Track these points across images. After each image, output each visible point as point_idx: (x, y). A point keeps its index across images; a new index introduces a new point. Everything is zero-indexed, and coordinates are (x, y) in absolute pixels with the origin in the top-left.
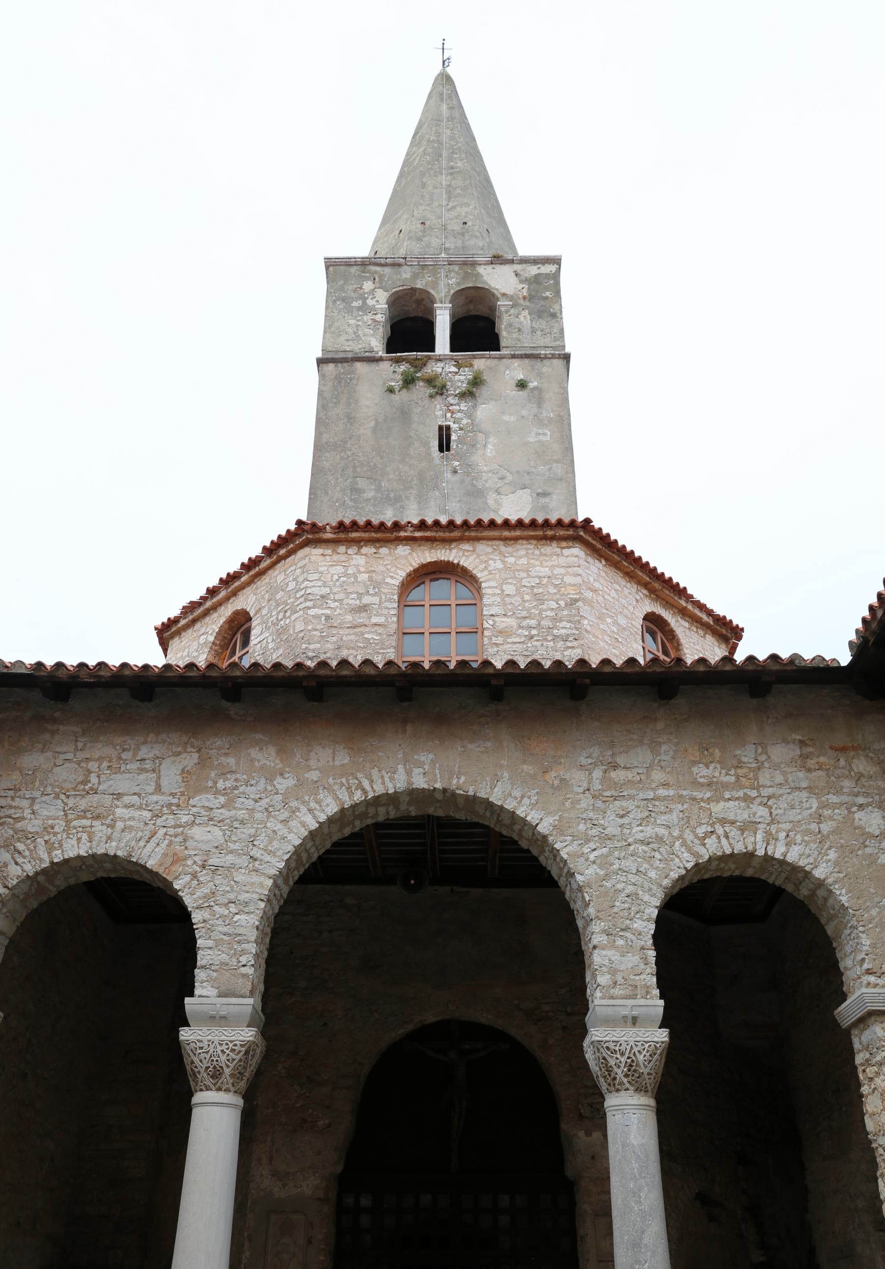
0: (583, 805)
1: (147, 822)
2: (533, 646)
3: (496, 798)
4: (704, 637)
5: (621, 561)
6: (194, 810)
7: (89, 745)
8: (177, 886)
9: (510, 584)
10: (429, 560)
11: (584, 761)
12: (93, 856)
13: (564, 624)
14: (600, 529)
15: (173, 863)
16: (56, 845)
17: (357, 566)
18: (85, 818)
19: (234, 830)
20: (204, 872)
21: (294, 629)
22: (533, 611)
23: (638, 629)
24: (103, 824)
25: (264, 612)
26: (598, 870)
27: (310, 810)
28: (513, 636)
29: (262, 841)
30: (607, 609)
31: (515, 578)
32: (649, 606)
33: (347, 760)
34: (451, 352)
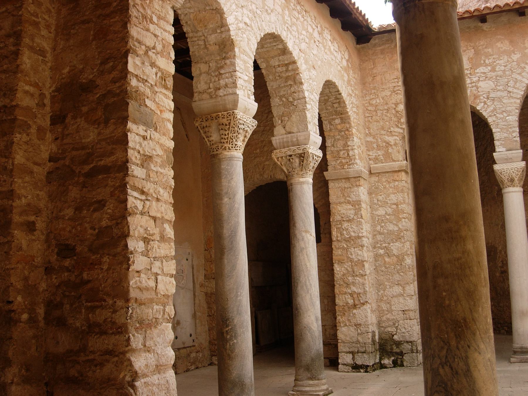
8: (478, 108)
15: (475, 99)
20: (489, 101)
29: (511, 83)
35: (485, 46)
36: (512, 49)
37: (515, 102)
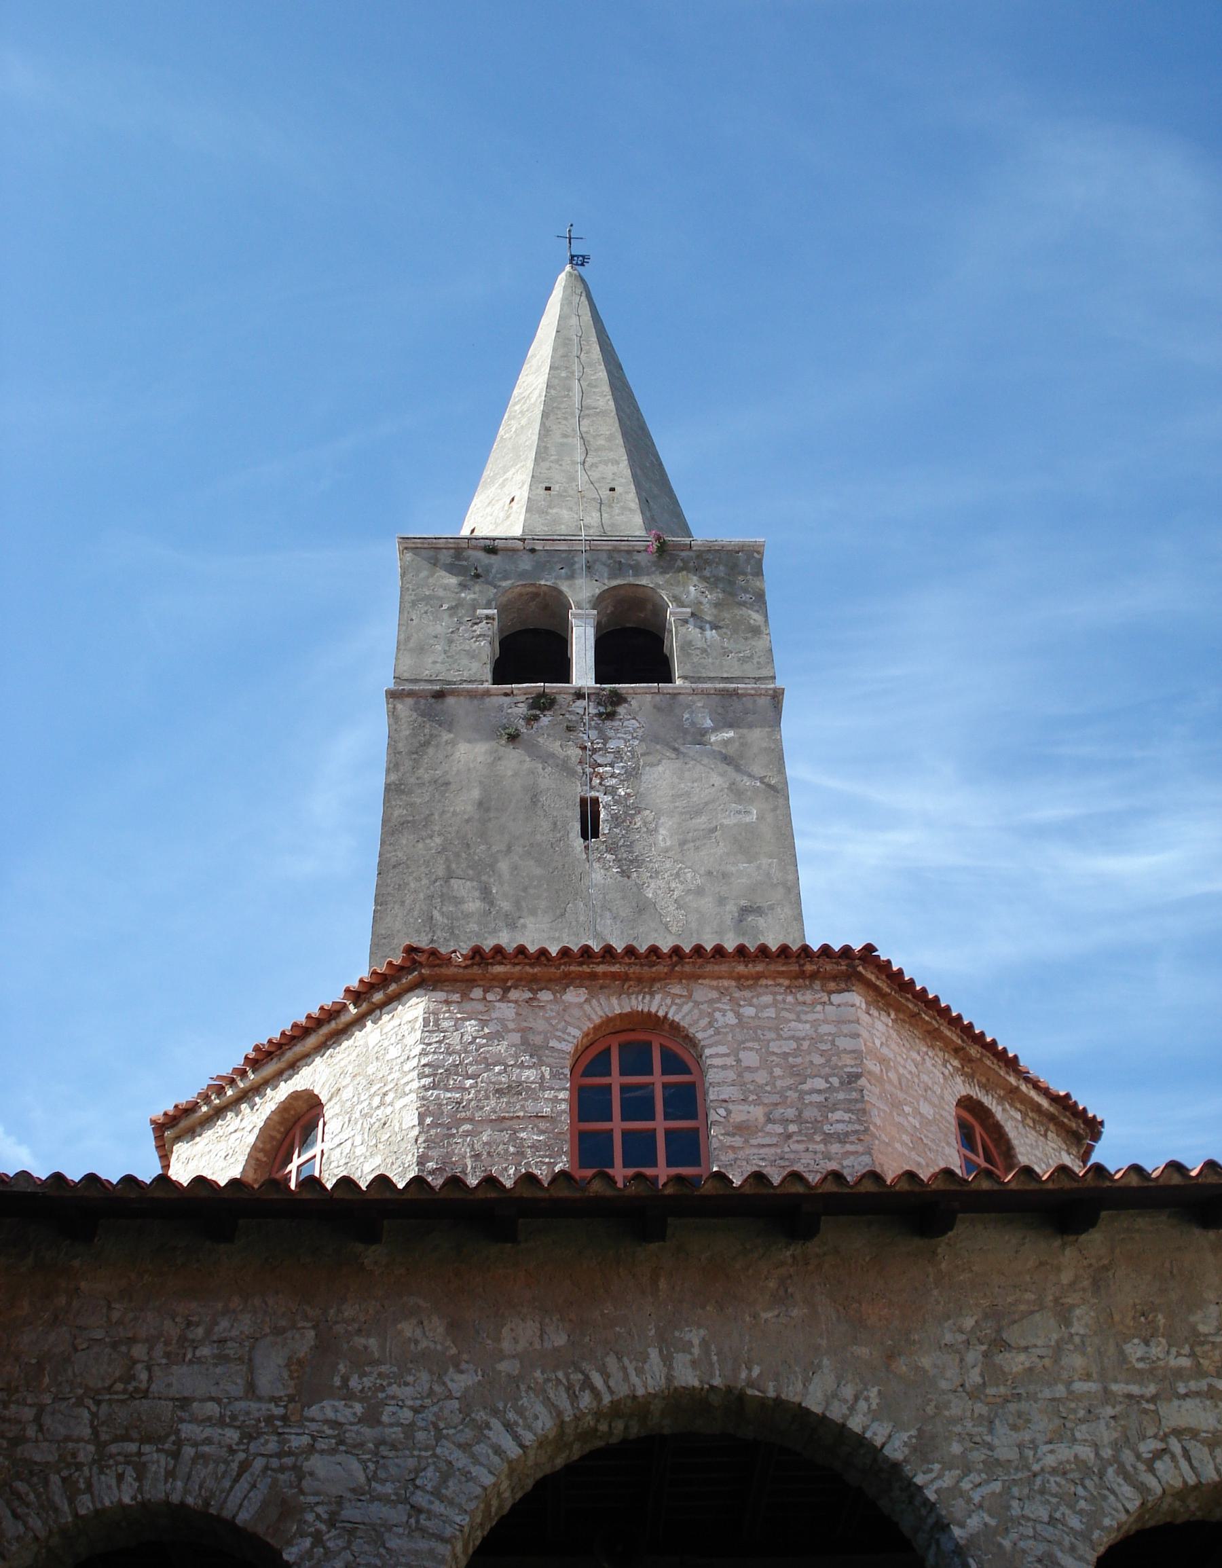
0: (955, 1411)
1: (235, 1447)
2: (792, 1151)
3: (814, 1403)
4: (1045, 1136)
5: (919, 1014)
6: (313, 1426)
7: (131, 1315)
9: (751, 1049)
10: (618, 1011)
11: (948, 1338)
12: (144, 1505)
13: (838, 1115)
14: (889, 962)
16: (82, 1486)
17: (501, 1021)
18: (126, 1438)
19: (381, 1462)
20: (334, 1532)
21: (401, 1124)
22: (789, 1093)
23: (949, 1123)
24: (158, 1451)
25: (346, 1094)
26: (987, 1519)
27: (509, 1427)
28: (760, 1134)
29: (429, 1478)
30: (901, 1089)
31: (758, 1040)
32: (962, 1088)
33: (560, 1340)
34: (596, 683)
35: (356, 1326)
36: (454, 1351)
37: (431, 1551)
